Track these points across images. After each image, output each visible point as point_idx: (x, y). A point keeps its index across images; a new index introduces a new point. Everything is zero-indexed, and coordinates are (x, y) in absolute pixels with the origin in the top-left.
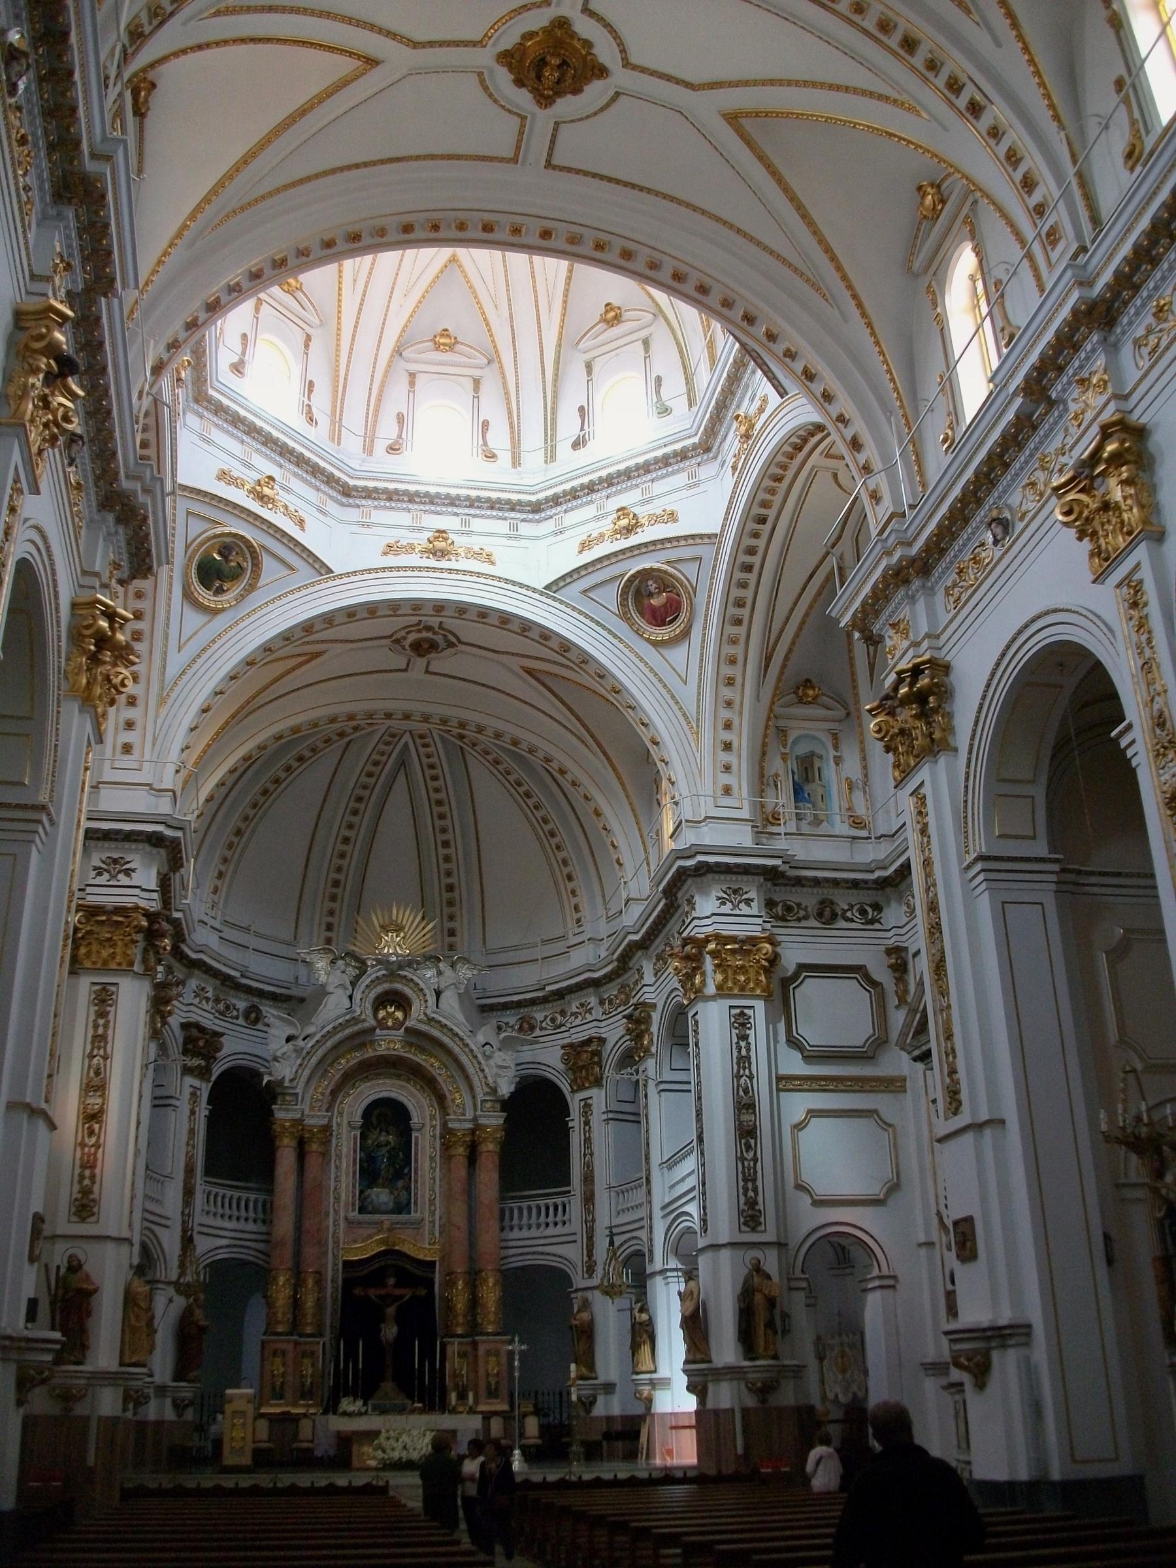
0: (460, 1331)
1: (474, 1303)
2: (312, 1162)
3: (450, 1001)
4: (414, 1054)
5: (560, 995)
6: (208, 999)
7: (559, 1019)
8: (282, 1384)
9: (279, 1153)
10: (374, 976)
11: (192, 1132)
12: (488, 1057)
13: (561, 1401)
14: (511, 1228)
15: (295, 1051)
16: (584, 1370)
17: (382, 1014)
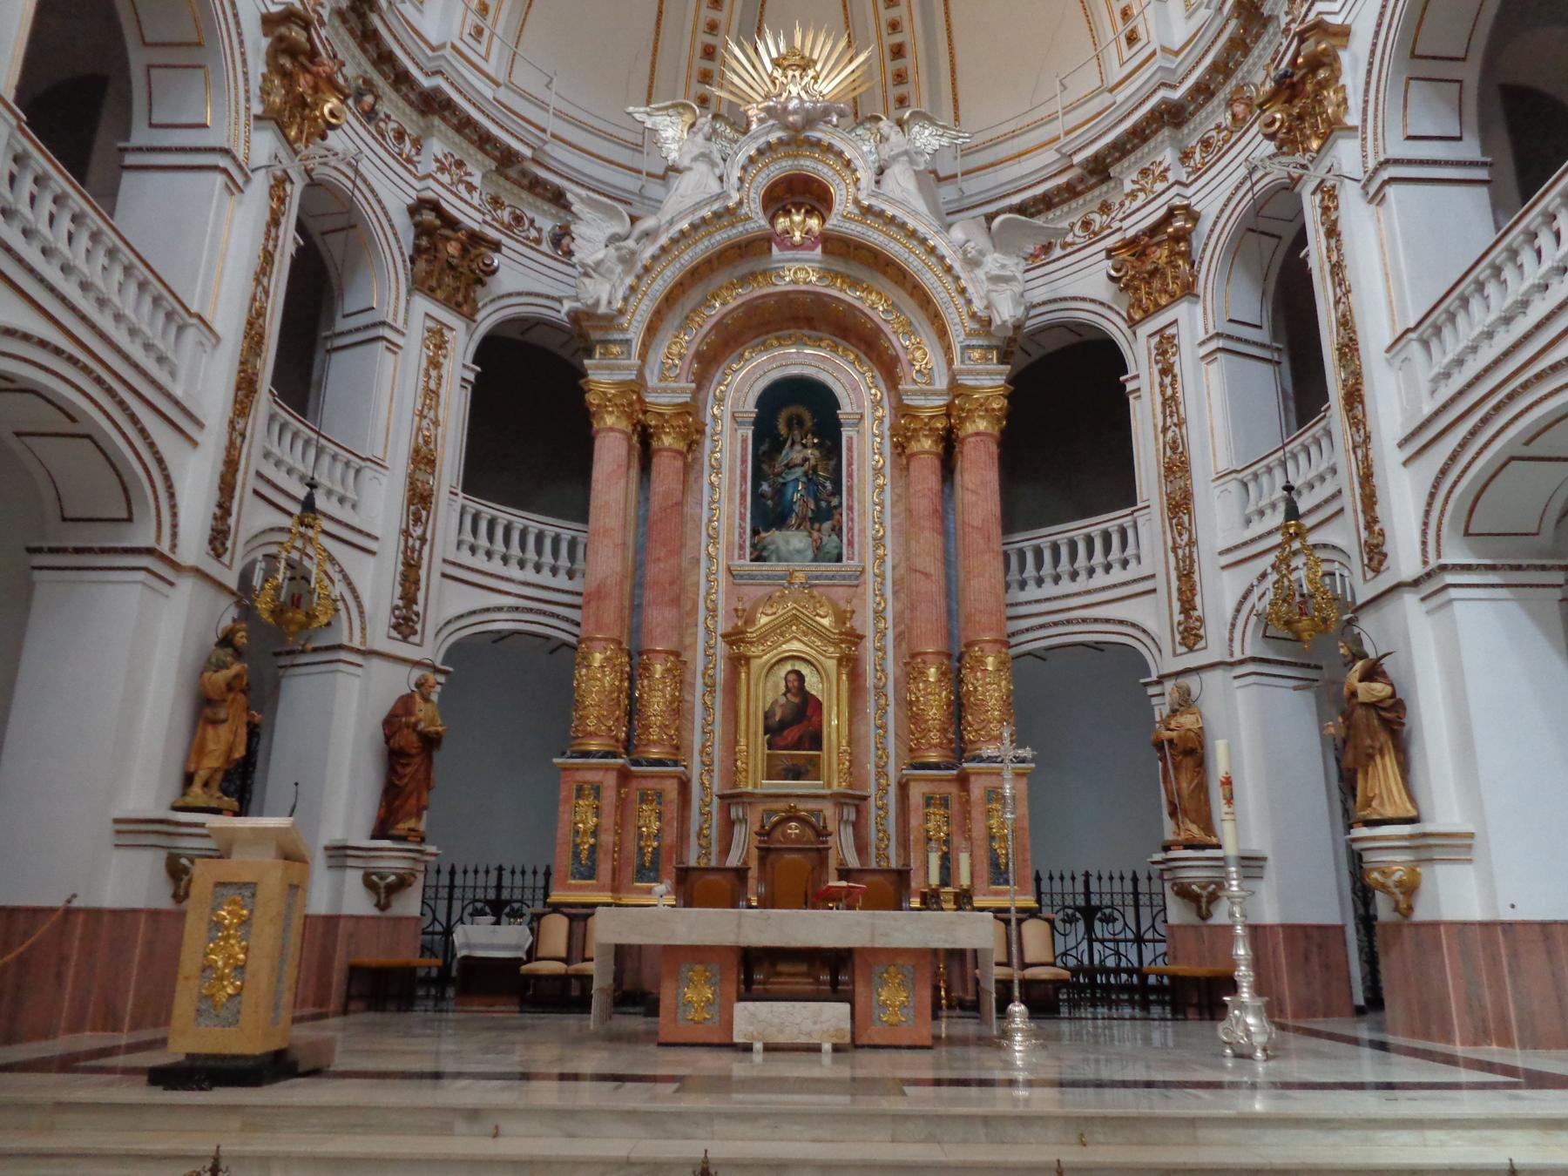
0: (933, 757)
1: (958, 708)
2: (666, 468)
3: (901, 181)
4: (841, 290)
5: (1099, 169)
6: (471, 188)
7: (1098, 220)
8: (593, 846)
9: (597, 444)
10: (762, 140)
11: (432, 395)
12: (973, 263)
13: (1136, 894)
14: (1023, 585)
15: (622, 260)
16: (1194, 828)
17: (782, 223)
